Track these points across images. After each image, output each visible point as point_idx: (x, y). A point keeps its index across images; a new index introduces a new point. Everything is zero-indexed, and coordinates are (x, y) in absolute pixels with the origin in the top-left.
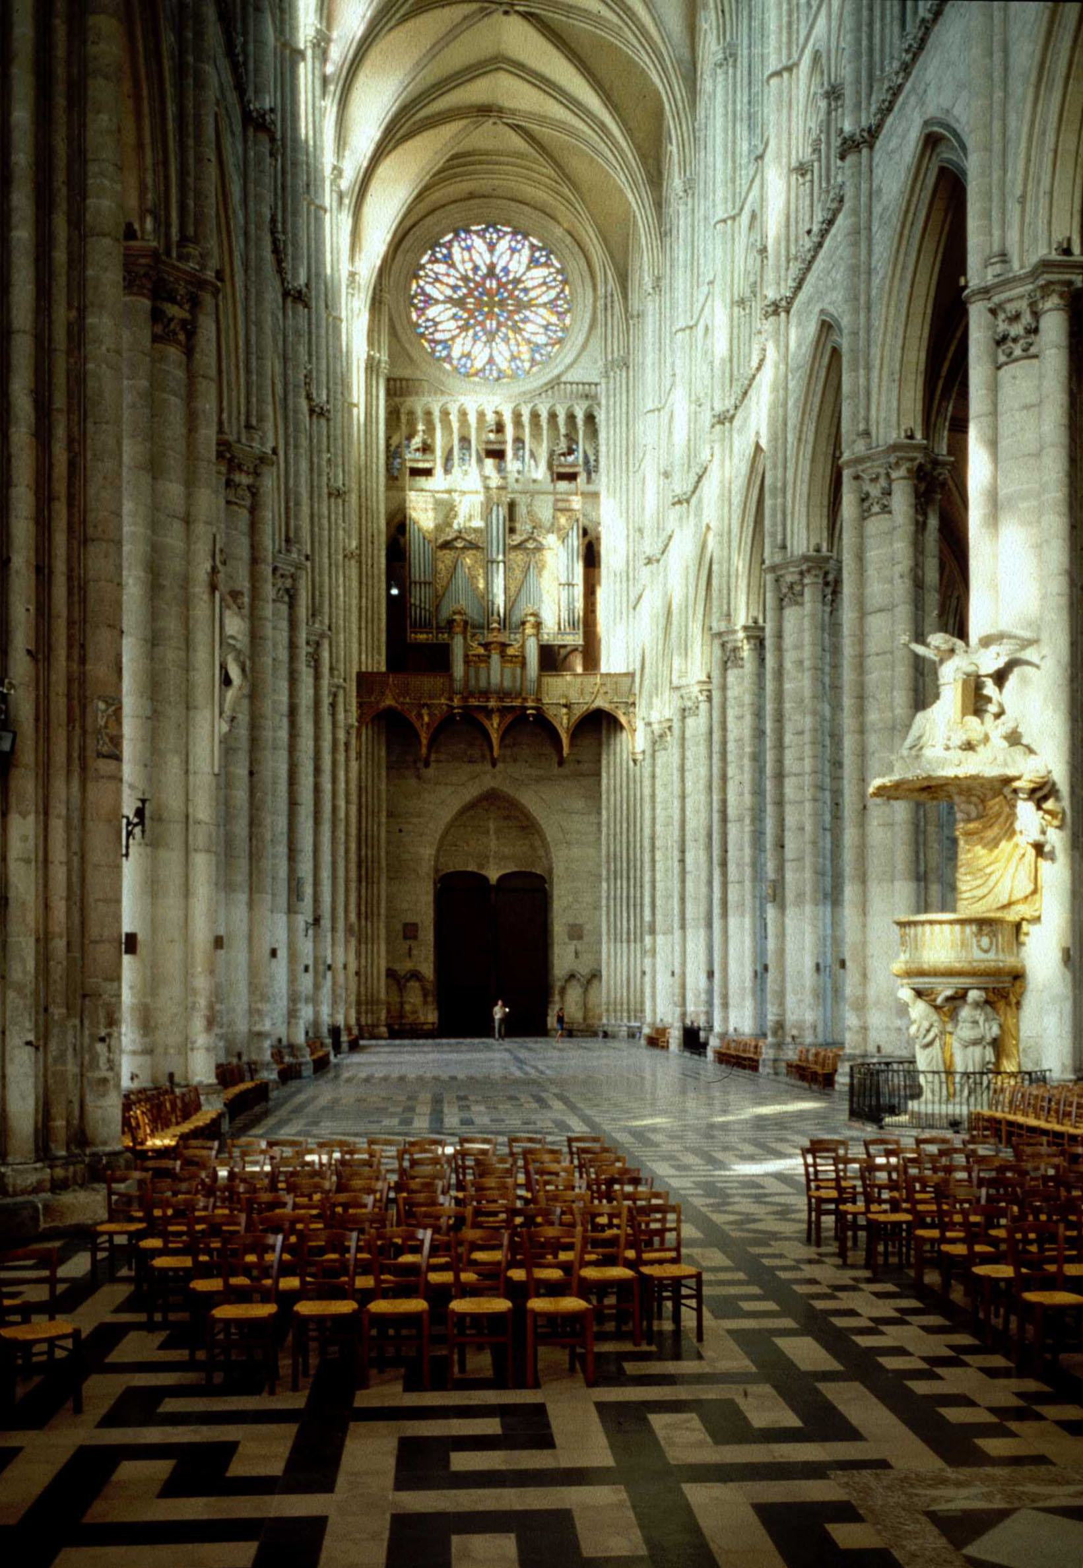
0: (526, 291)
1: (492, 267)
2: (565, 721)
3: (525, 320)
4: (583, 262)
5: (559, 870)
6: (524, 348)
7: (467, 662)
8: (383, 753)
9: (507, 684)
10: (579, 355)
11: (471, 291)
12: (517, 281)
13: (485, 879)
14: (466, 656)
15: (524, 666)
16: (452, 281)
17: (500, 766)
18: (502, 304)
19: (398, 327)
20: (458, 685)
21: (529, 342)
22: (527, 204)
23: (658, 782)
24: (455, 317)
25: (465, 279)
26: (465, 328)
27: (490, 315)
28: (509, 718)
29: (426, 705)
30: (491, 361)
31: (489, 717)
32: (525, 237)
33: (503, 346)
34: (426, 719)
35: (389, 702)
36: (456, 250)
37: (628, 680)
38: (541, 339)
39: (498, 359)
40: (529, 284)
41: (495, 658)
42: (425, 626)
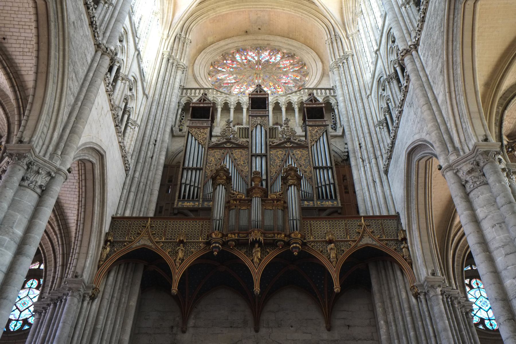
0: (279, 68)
2: (333, 255)
4: (315, 54)
7: (228, 207)
8: (133, 303)
9: (269, 222)
14: (228, 202)
15: (285, 208)
16: (234, 66)
17: (263, 331)
19: (199, 79)
20: (216, 224)
22: (279, 36)
23: (486, 226)
28: (272, 254)
29: (182, 242)
31: (250, 254)
32: (278, 51)
34: (180, 255)
35: (143, 242)
36: (238, 57)
37: (392, 223)
41: (256, 202)
42: (195, 198)
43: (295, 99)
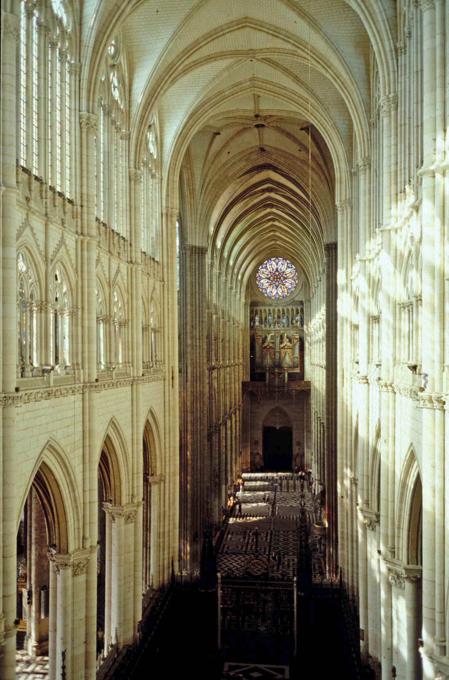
0: (286, 275)
1: (277, 269)
3: (286, 282)
5: (294, 427)
6: (285, 289)
10: (300, 292)
11: (272, 276)
12: (284, 272)
13: (275, 428)
18: (280, 278)
21: (286, 288)
24: (268, 282)
25: (270, 272)
26: (270, 285)
27: (277, 281)
30: (277, 293)
33: (280, 289)
38: (290, 287)
39: (279, 293)
40: (287, 273)
43: (290, 308)
